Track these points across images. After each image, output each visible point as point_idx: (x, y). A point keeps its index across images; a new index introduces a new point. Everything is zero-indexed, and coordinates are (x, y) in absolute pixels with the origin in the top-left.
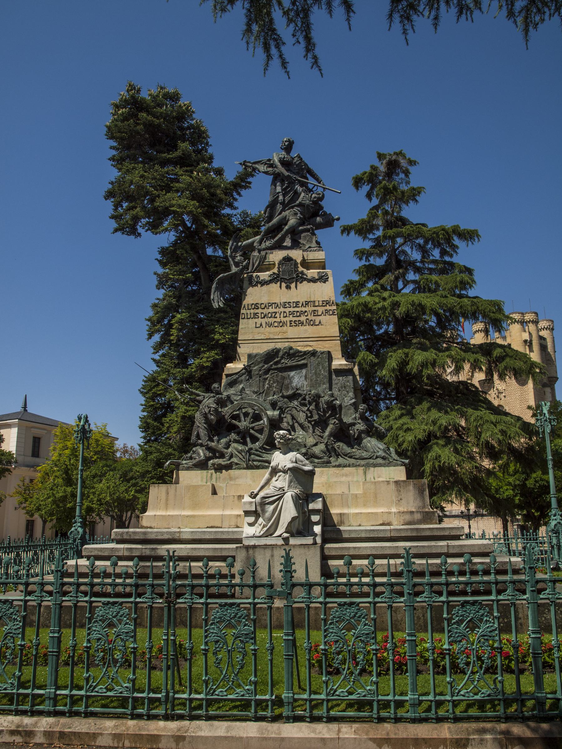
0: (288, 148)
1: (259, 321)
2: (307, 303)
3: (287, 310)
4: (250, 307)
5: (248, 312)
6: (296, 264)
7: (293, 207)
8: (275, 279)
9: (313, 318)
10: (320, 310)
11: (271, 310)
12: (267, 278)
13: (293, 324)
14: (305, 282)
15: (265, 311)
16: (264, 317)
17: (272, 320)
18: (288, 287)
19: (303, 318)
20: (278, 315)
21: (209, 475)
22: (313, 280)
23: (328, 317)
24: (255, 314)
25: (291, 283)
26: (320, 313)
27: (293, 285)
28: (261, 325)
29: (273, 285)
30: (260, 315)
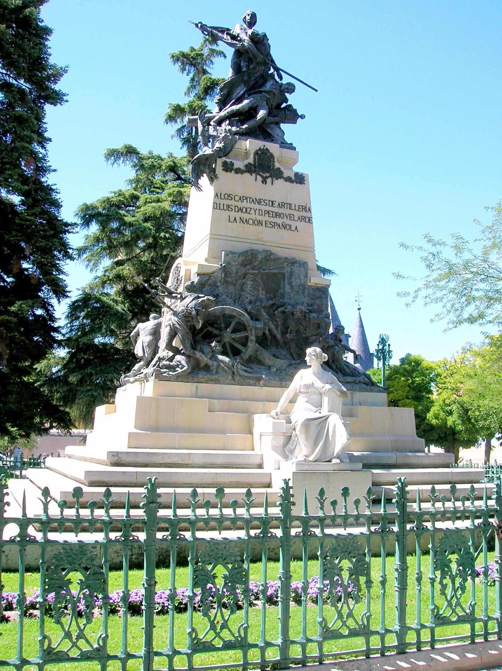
0: (252, 21)
1: (233, 214)
2: (281, 205)
3: (264, 208)
4: (223, 197)
5: (222, 202)
6: (272, 156)
7: (260, 92)
8: (249, 169)
9: (290, 222)
10: (297, 214)
11: (245, 204)
12: (242, 167)
13: (269, 225)
14: (282, 180)
15: (239, 204)
16: (238, 211)
17: (245, 216)
18: (264, 181)
19: (279, 221)
20: (252, 212)
21: (195, 388)
22: (288, 179)
23: (303, 223)
24: (228, 206)
25: (267, 177)
26: (296, 218)
27: (269, 180)
28: (235, 219)
29: (247, 175)
30: (233, 208)
